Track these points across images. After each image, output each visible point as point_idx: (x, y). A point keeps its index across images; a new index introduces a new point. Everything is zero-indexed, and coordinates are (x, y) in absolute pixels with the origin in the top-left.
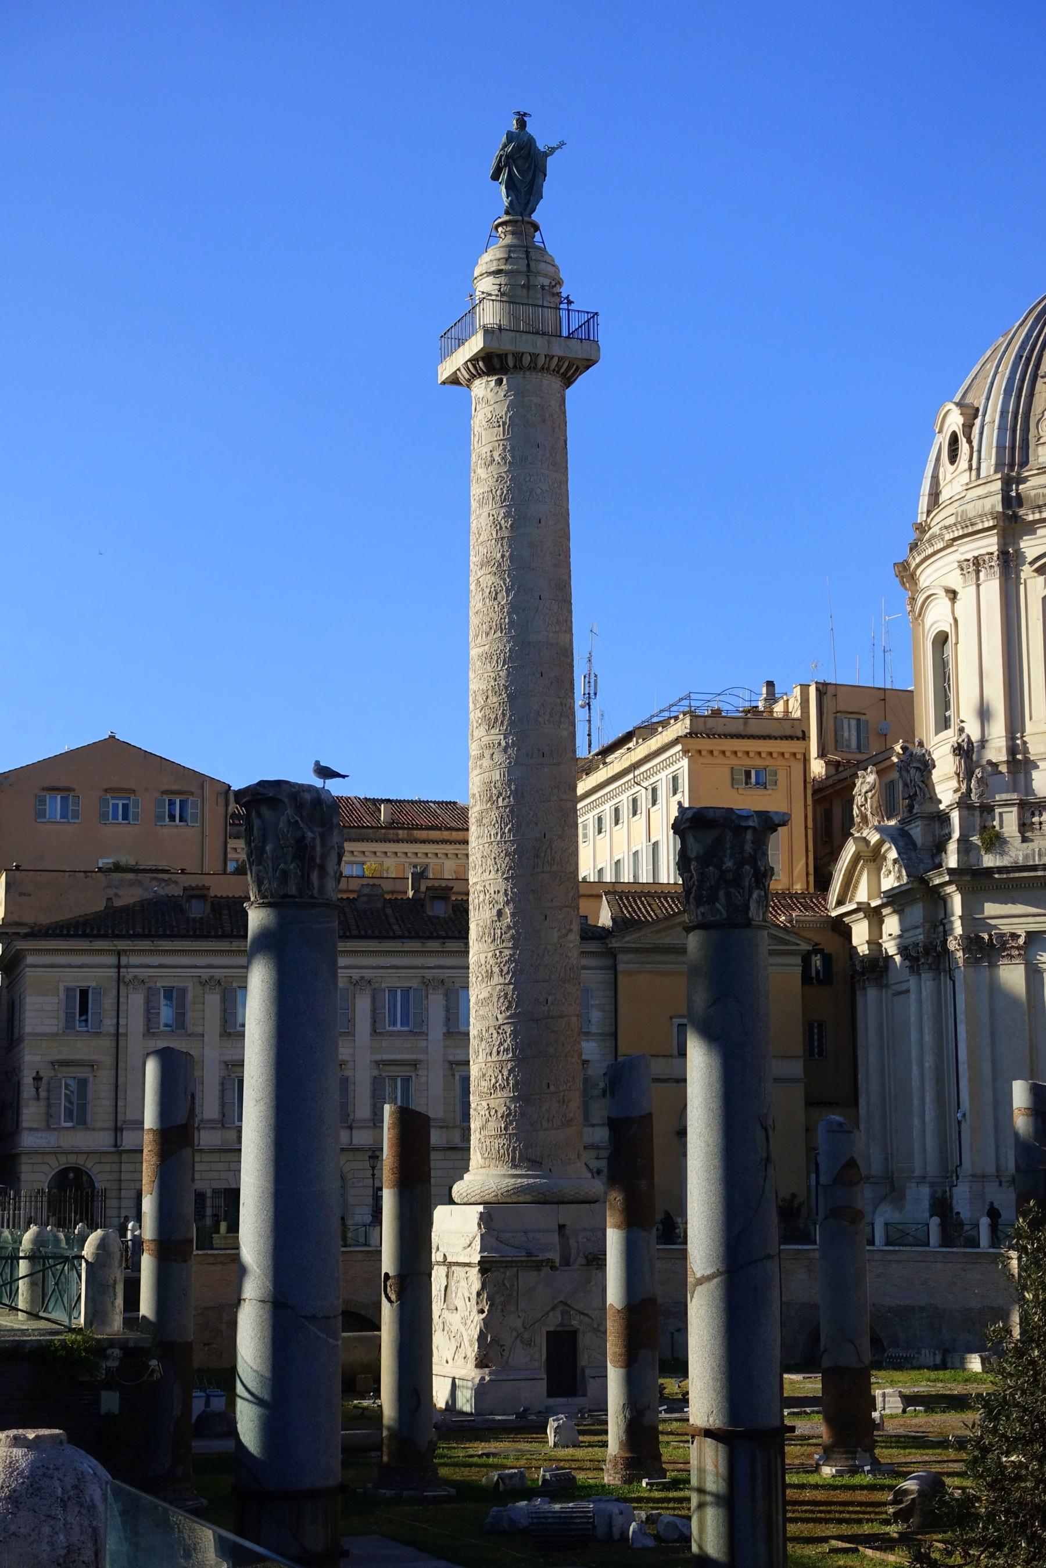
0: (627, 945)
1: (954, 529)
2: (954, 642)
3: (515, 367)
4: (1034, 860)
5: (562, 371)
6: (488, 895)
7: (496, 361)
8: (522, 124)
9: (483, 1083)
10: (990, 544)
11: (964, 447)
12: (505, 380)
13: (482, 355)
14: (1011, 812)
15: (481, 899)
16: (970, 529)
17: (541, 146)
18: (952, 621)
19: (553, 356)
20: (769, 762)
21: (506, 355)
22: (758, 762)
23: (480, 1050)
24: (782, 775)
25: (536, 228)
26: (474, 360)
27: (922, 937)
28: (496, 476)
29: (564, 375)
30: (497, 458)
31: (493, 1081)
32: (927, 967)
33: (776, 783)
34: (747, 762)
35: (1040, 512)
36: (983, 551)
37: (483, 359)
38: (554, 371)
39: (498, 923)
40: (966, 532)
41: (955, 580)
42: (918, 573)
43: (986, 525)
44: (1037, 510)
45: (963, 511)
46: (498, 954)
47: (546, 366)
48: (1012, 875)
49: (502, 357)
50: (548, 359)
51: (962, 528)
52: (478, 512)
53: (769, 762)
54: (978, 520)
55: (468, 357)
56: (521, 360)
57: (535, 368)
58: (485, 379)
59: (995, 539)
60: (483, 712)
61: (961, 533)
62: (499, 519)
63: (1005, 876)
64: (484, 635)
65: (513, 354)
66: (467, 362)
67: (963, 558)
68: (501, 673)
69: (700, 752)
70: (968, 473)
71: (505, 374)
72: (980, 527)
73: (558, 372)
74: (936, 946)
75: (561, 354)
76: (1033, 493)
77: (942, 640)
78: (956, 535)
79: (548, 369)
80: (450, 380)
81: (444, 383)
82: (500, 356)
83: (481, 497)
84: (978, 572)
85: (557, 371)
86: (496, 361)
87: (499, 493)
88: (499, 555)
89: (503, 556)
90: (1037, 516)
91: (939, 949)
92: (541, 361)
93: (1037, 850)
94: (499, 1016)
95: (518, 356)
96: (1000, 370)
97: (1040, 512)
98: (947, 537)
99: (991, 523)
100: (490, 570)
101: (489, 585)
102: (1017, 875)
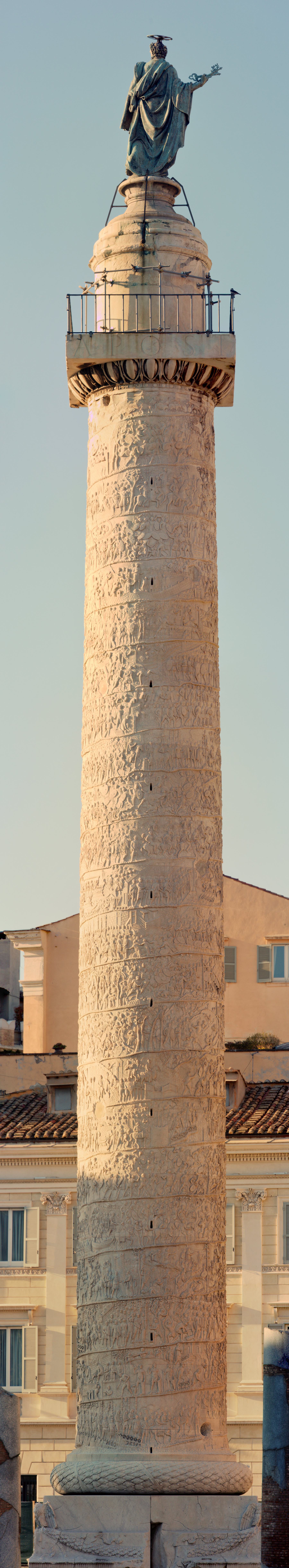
8: (160, 51)
17: (184, 76)
19: (168, 361)
21: (105, 364)
25: (175, 190)
28: (100, 527)
38: (175, 378)
47: (161, 374)
50: (161, 365)
57: (146, 379)
65: (113, 363)
68: (101, 788)
75: (180, 356)
79: (165, 377)
92: (152, 368)
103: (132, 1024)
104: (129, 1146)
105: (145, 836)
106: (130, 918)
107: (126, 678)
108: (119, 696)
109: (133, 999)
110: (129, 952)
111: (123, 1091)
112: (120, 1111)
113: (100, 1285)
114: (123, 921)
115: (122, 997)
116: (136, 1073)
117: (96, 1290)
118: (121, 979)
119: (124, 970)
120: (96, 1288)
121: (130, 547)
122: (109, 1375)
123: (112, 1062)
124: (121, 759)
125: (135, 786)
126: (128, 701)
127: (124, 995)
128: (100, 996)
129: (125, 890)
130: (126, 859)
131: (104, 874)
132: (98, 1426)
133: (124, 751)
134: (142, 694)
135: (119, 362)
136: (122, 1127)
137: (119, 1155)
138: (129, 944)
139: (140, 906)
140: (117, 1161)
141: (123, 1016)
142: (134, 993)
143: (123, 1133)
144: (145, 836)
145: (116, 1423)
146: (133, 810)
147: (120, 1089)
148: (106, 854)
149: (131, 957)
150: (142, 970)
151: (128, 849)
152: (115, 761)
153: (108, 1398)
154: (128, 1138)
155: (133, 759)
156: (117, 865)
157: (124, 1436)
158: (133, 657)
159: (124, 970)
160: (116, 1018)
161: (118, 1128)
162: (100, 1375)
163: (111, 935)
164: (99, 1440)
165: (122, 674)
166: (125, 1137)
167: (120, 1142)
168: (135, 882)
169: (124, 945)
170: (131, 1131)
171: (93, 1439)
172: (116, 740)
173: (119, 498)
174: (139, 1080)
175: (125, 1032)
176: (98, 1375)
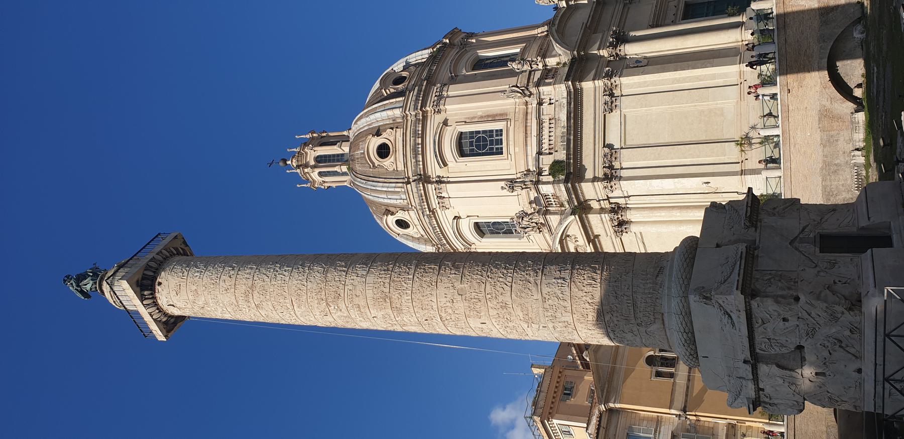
0: (604, 396)
2: (477, 217)
3: (154, 272)
5: (175, 252)
6: (448, 304)
7: (145, 282)
10: (431, 187)
11: (400, 215)
12: (160, 280)
13: (138, 289)
14: (542, 159)
15: (450, 311)
16: (424, 198)
18: (469, 218)
20: (562, 384)
21: (144, 274)
22: (561, 388)
23: (563, 319)
24: (569, 380)
26: (142, 298)
27: (606, 215)
29: (179, 254)
30: (194, 288)
31: (587, 305)
33: (571, 382)
34: (559, 393)
35: (419, 161)
36: (434, 191)
37: (142, 290)
39: (468, 295)
40: (425, 200)
43: (422, 188)
44: (418, 163)
45: (419, 205)
46: (489, 296)
48: (572, 153)
49: (144, 277)
51: (423, 202)
52: (221, 305)
53: (562, 384)
55: (141, 304)
56: (152, 267)
58: (157, 295)
60: (330, 304)
61: (425, 204)
62: (225, 286)
63: (572, 156)
64: (287, 301)
65: (145, 270)
66: (143, 305)
67: (438, 206)
68: (308, 287)
69: (550, 413)
71: (156, 280)
72: (422, 192)
73: (174, 254)
74: (612, 207)
76: (413, 168)
77: (477, 226)
78: (426, 207)
80: (164, 331)
81: (166, 336)
82: (143, 279)
83: (213, 300)
84: (444, 197)
85: (172, 255)
86: (145, 282)
87: (212, 286)
88: (244, 287)
89: (245, 284)
90: (421, 163)
91: (613, 206)
93: (562, 143)
94: (535, 297)
95: (148, 267)
96: (369, 194)
97: (419, 161)
99: (421, 185)
100: (250, 295)
101: (258, 295)
102: (572, 150)
103: (423, 269)
104: (485, 271)
105: (339, 264)
106: (372, 270)
107: (268, 272)
108: (273, 276)
109: (411, 268)
110: (388, 270)
111: (455, 274)
112: (465, 276)
113: (560, 292)
114: (373, 273)
115: (409, 274)
116: (448, 267)
117: (562, 295)
118: (399, 275)
119: (396, 272)
120: (561, 295)
121: (217, 271)
122: (616, 286)
123: (439, 280)
124: (300, 275)
125: (315, 268)
126: (277, 271)
127: (408, 273)
128: (405, 289)
129: (359, 272)
130: (344, 271)
131: (347, 285)
132: (649, 296)
133: (297, 273)
134: (278, 265)
135: (146, 267)
136: (474, 274)
137: (488, 277)
138: (384, 270)
139: (369, 266)
140: (491, 278)
141: (418, 273)
142: (409, 268)
143: (477, 274)
144: (339, 264)
145: (648, 282)
146: (324, 268)
147: (454, 275)
148: (338, 284)
149: (391, 269)
150: (400, 264)
151: (340, 271)
152: (300, 278)
153: (631, 288)
154: (480, 272)
155: (303, 269)
156: (346, 276)
157: (657, 276)
158: (261, 269)
159: (396, 272)
160: (418, 278)
161: (474, 277)
162: (616, 293)
163: (377, 280)
164: (659, 295)
165: (265, 274)
166: (479, 273)
167: (482, 276)
168: (358, 267)
169: (384, 272)
170: (478, 270)
171: (658, 300)
172: (291, 277)
173: (197, 276)
174: (453, 266)
175: (427, 273)
176: (615, 295)
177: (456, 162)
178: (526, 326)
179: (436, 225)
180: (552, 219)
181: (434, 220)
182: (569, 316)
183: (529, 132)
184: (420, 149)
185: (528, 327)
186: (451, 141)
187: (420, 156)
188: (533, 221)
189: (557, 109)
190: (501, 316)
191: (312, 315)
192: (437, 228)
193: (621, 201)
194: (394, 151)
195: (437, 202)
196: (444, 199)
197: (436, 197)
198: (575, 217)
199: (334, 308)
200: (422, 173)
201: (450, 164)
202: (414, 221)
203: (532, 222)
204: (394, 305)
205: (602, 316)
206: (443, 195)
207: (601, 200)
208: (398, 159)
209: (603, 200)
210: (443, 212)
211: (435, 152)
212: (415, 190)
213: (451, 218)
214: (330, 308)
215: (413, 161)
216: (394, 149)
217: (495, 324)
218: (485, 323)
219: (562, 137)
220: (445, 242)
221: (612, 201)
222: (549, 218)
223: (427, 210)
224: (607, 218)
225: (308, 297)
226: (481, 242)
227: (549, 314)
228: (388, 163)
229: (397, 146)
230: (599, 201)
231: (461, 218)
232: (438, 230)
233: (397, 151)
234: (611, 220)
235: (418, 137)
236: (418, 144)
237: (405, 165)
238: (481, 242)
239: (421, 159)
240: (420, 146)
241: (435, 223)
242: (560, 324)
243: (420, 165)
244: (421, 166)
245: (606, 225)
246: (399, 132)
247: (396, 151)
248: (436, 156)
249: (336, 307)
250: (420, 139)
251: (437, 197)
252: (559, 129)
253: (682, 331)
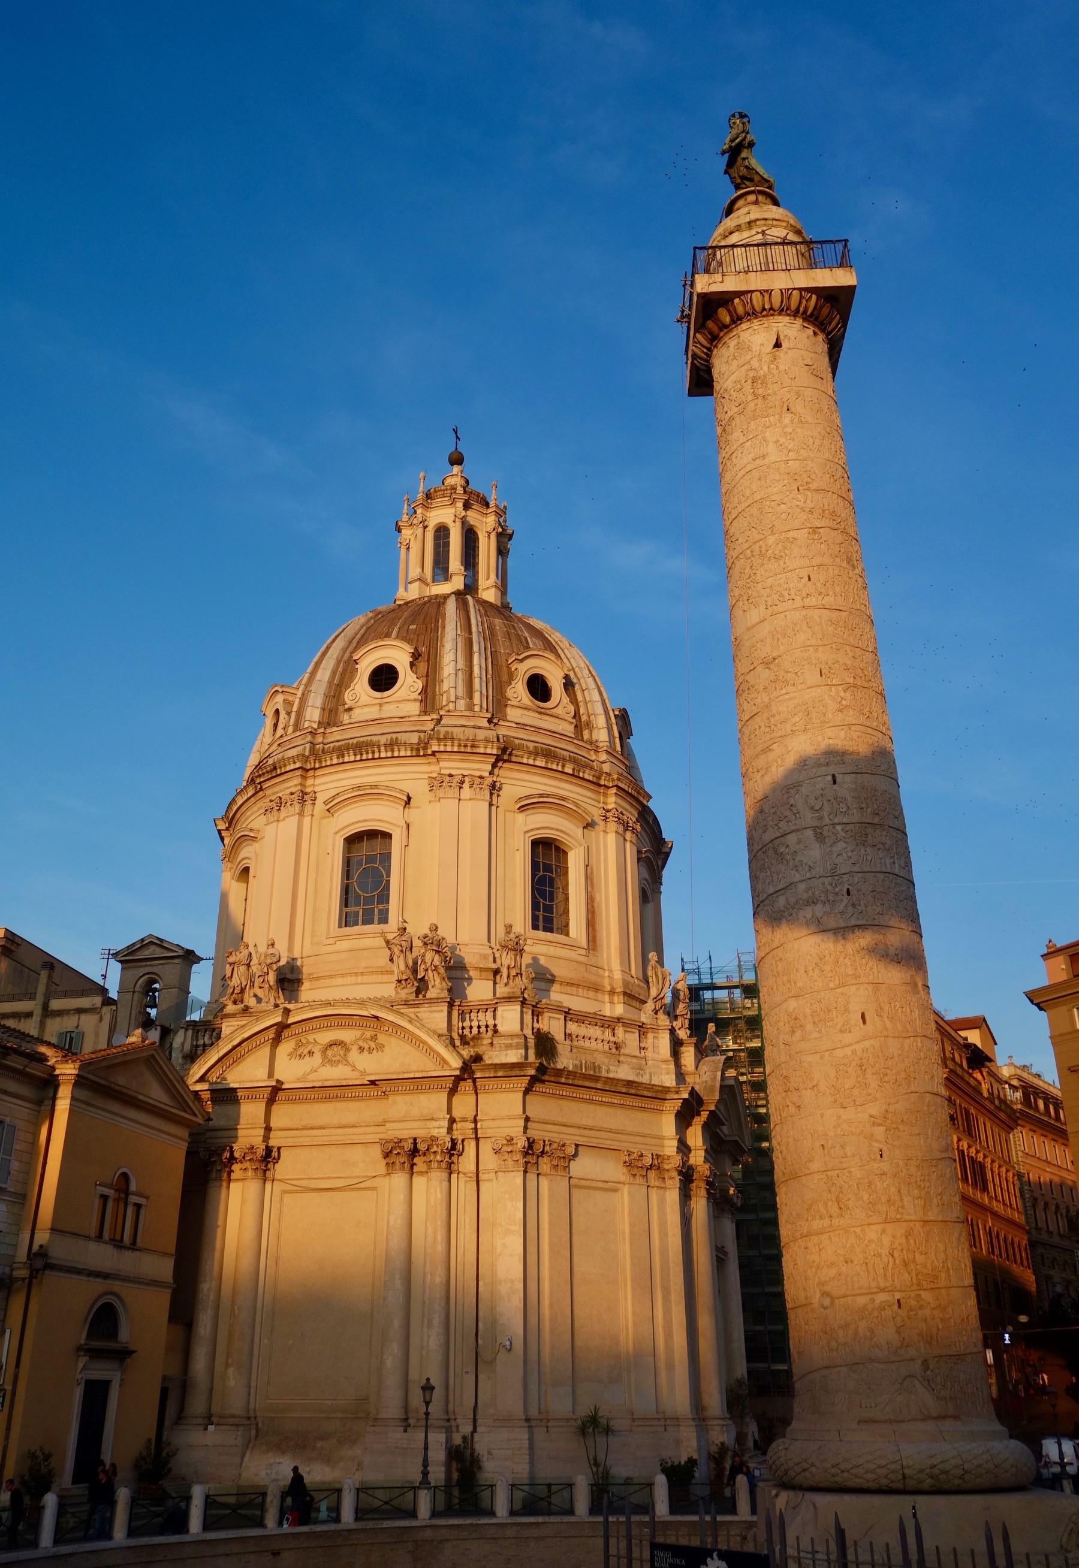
1: (449, 743)
4: (582, 1069)
9: (920, 1258)
11: (409, 683)
14: (559, 1019)
16: (469, 750)
18: (405, 826)
32: (444, 1165)
36: (478, 774)
40: (462, 750)
41: (419, 788)
42: (319, 772)
43: (489, 751)
45: (447, 732)
51: (460, 745)
54: (482, 744)
59: (489, 767)
61: (456, 749)
67: (447, 772)
70: (418, 704)
72: (482, 750)
76: (517, 741)
78: (449, 749)
90: (531, 762)
97: (534, 759)
98: (435, 748)
99: (495, 752)
177: (526, 832)
178: (874, 1112)
179: (396, 754)
180: (436, 1015)
181: (409, 753)
182: (916, 1213)
183: (568, 989)
184: (554, 767)
185: (871, 1116)
186: (561, 831)
187: (543, 764)
188: (430, 972)
189: (634, 1060)
190: (890, 1062)
191: (813, 642)
192: (389, 754)
193: (467, 1162)
194: (539, 710)
195: (453, 772)
196: (458, 788)
197: (466, 773)
198: (457, 1069)
199: (842, 698)
200: (514, 759)
201: (521, 817)
202: (394, 706)
203: (427, 970)
204: (870, 830)
205: (929, 1287)
206: (466, 786)
207: (476, 1125)
208: (526, 712)
209: (476, 1129)
210: (426, 776)
211: (548, 796)
212: (481, 734)
213: (408, 787)
214: (840, 688)
215: (531, 745)
216: (542, 710)
217: (867, 1044)
218: (864, 1022)
219: (594, 1063)
220: (346, 759)
221: (470, 1148)
222: (441, 1008)
223: (442, 749)
224: (436, 1131)
225: (853, 649)
226: (336, 833)
227: (913, 1169)
228: (519, 691)
229: (549, 718)
230: (475, 1121)
231: (405, 807)
232: (383, 755)
233: (539, 716)
234: (434, 1139)
235: (574, 769)
236: (563, 766)
237: (522, 726)
238: (336, 833)
239: (538, 763)
240: (560, 768)
241: (402, 753)
242: (893, 1189)
243: (528, 758)
244: (525, 761)
245: (416, 1124)
246: (569, 729)
247: (541, 713)
248: (541, 795)
249: (844, 702)
250: (571, 772)
251: (464, 776)
252: (606, 1060)
253: (967, 1466)
